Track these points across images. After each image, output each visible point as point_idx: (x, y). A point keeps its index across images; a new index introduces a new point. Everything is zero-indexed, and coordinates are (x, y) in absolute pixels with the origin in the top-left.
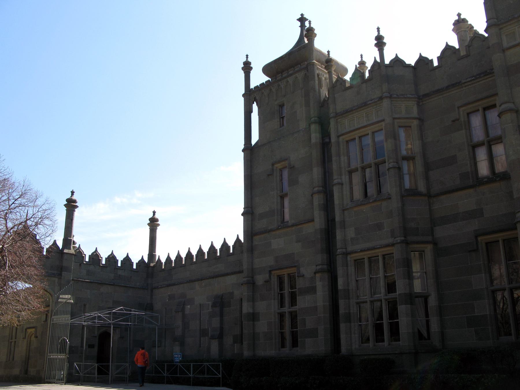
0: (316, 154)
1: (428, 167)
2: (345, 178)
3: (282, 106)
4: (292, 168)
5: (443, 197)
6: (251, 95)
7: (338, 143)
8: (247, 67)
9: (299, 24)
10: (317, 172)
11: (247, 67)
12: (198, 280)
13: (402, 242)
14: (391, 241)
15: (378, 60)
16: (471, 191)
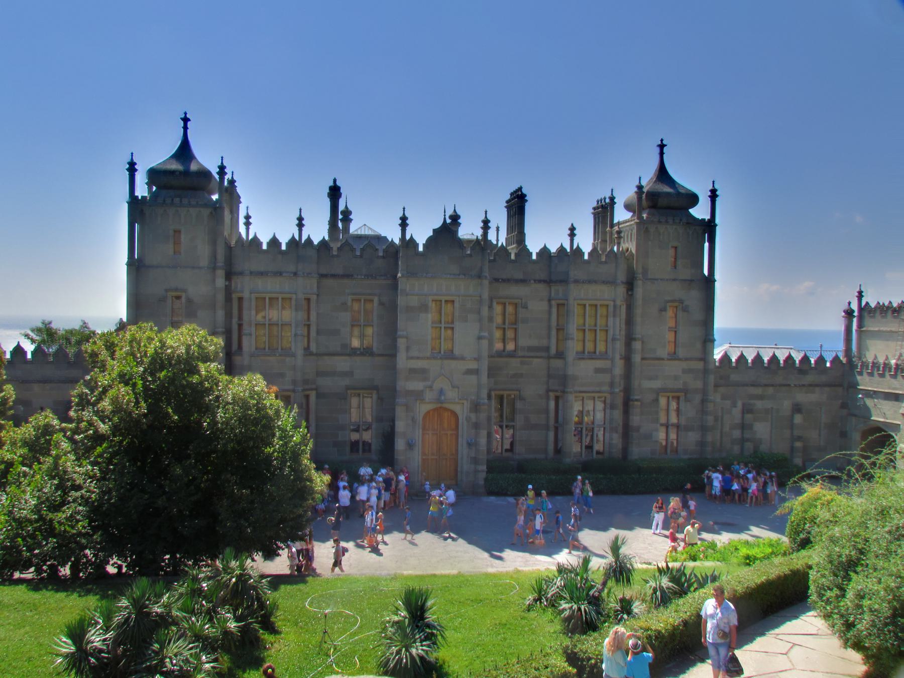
0: (221, 297)
1: (318, 333)
2: (253, 329)
3: (177, 232)
4: (189, 301)
5: (326, 358)
6: (135, 204)
7: (250, 299)
8: (132, 169)
9: (182, 122)
10: (220, 314)
11: (132, 169)
12: (39, 382)
13: (304, 390)
14: (291, 387)
15: (297, 238)
16: (347, 358)
